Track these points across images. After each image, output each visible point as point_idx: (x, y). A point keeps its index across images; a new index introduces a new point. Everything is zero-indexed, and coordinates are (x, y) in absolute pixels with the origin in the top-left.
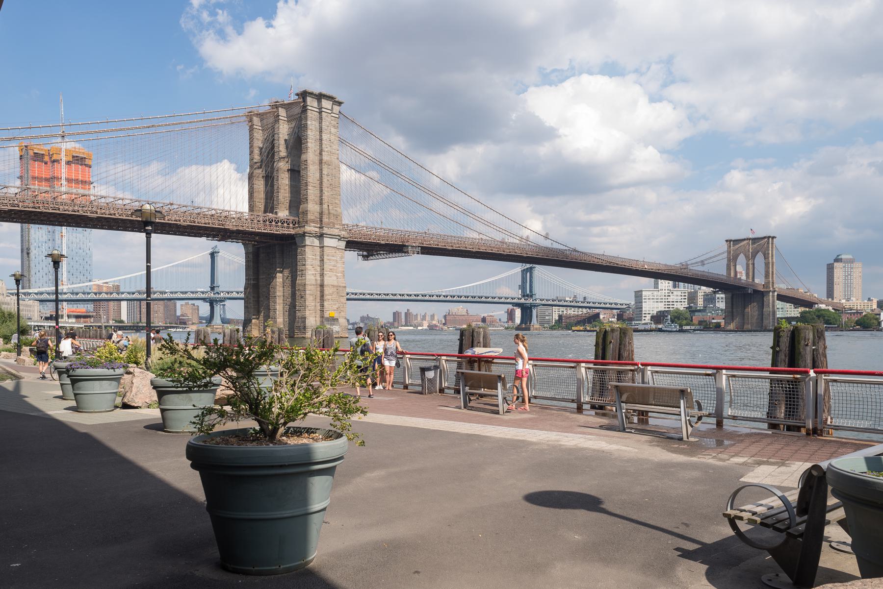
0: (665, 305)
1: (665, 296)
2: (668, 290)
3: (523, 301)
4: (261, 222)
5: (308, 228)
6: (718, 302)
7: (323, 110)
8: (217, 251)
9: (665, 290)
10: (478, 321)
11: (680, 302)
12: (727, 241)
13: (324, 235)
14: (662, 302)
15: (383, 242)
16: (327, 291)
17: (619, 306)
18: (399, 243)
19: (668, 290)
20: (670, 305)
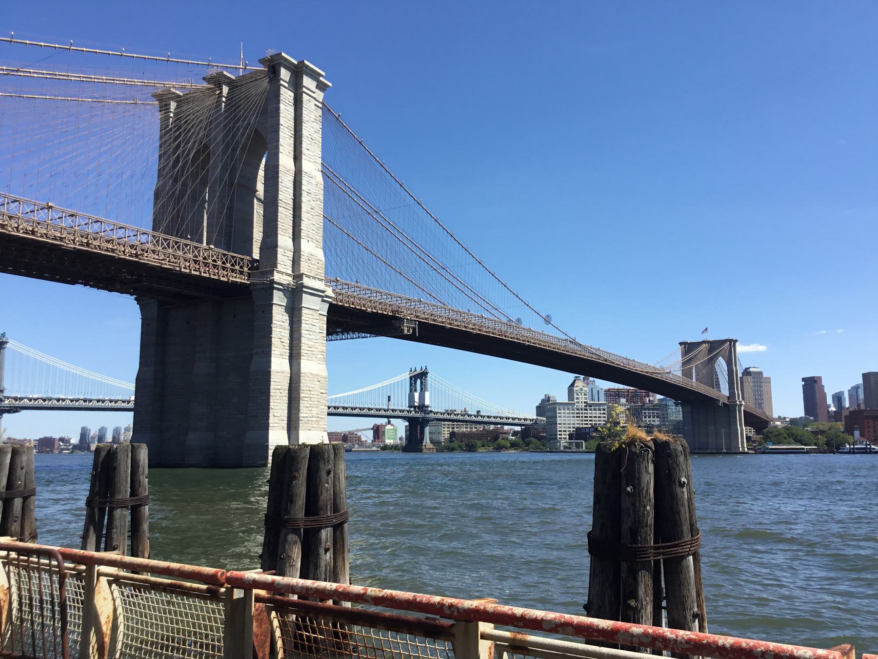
0: (582, 420)
1: (582, 410)
2: (585, 402)
3: (413, 414)
4: (201, 258)
5: (277, 277)
6: (645, 417)
7: (304, 89)
8: (4, 340)
9: (582, 402)
10: (339, 441)
11: (599, 417)
12: (681, 344)
13: (304, 289)
14: (579, 417)
15: (369, 310)
16: (305, 384)
17: (523, 422)
18: (390, 314)
19: (585, 402)
20: (587, 420)
